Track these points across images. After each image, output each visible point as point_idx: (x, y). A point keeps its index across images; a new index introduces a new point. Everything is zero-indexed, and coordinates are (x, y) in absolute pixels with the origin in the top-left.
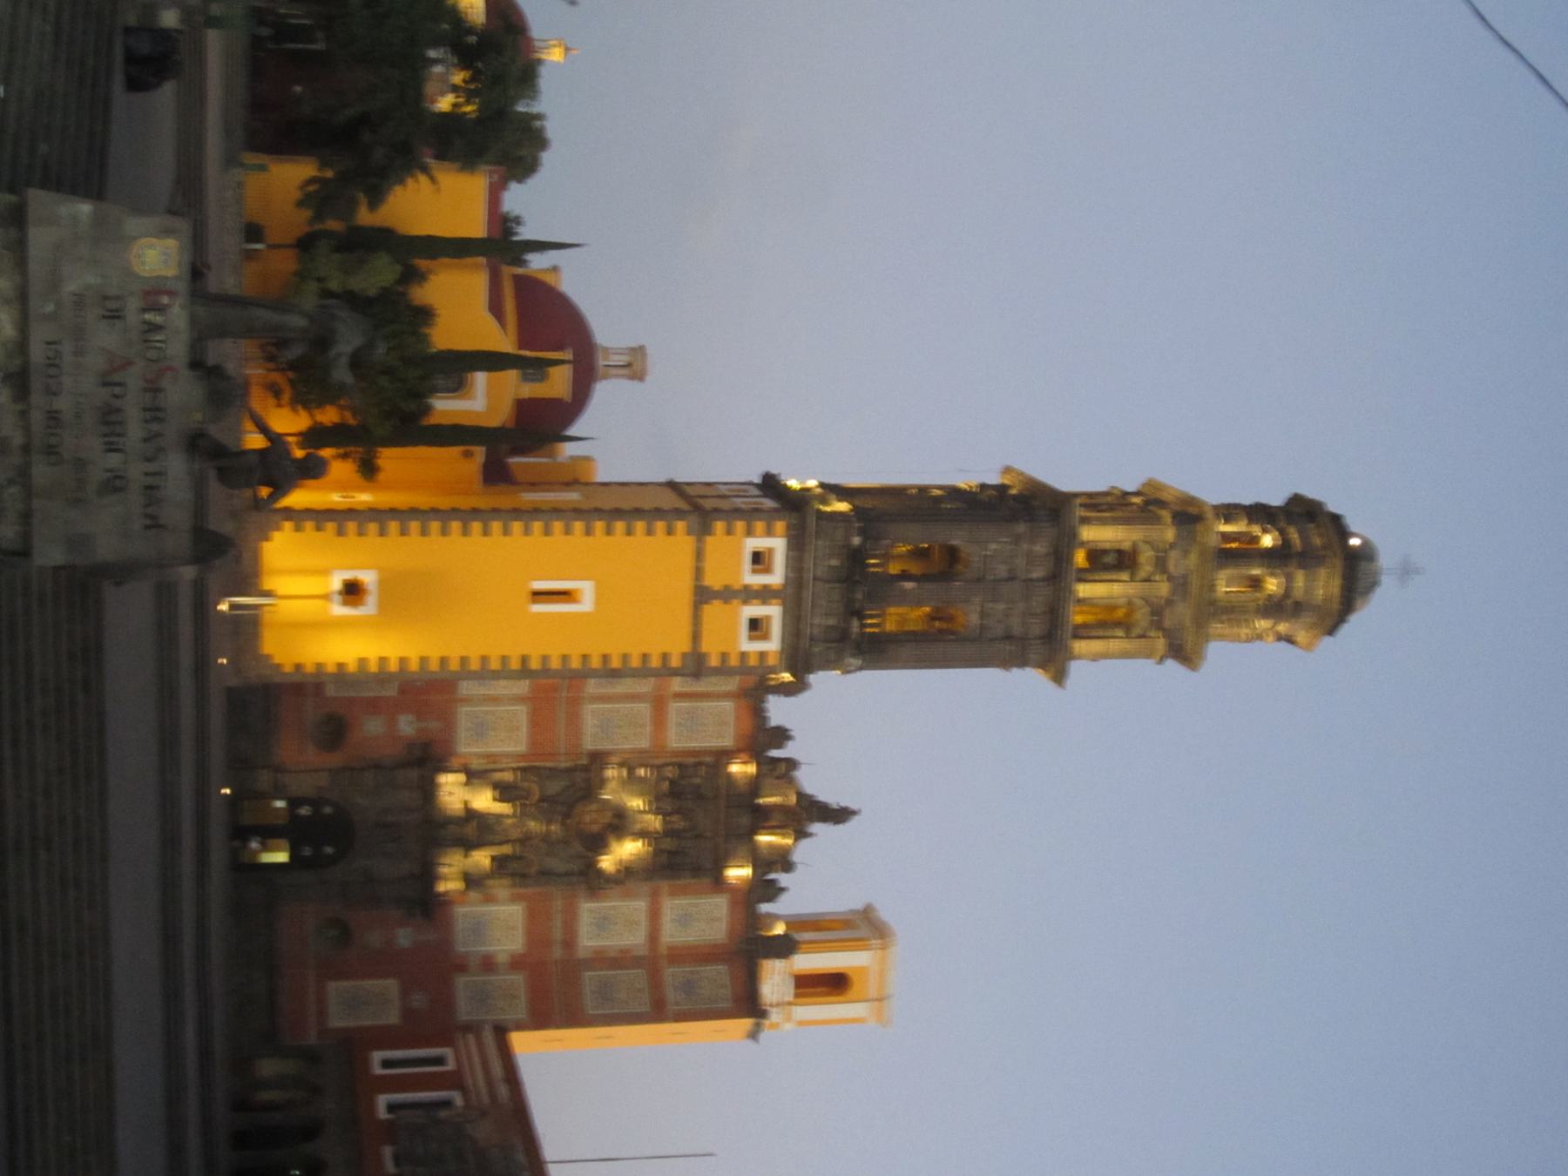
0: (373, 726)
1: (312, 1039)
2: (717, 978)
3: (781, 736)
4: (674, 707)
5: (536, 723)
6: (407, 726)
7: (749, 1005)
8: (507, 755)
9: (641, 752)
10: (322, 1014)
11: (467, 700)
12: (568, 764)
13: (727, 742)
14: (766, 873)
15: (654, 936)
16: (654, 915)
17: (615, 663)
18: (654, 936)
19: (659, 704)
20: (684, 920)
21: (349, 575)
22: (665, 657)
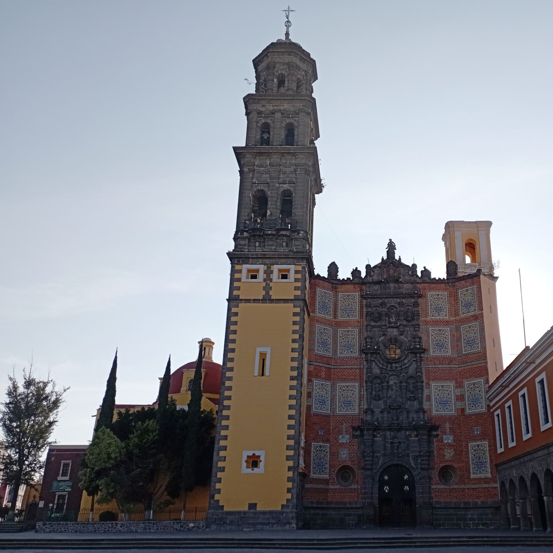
0: (344, 455)
1: (498, 485)
2: (465, 293)
3: (356, 272)
4: (340, 319)
5: (345, 380)
6: (344, 439)
7: (474, 277)
8: (360, 392)
9: (360, 332)
10: (486, 481)
11: (333, 410)
12: (365, 363)
13: (357, 294)
14: (417, 276)
15: (447, 323)
16: (436, 323)
17: (297, 336)
18: (447, 323)
19: (338, 324)
20: (438, 310)
21: (244, 464)
22: (295, 314)
